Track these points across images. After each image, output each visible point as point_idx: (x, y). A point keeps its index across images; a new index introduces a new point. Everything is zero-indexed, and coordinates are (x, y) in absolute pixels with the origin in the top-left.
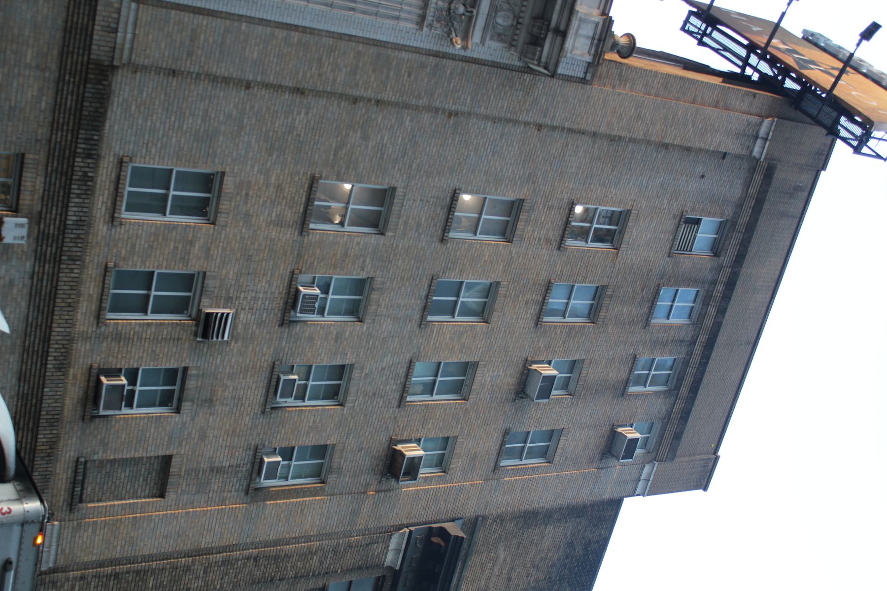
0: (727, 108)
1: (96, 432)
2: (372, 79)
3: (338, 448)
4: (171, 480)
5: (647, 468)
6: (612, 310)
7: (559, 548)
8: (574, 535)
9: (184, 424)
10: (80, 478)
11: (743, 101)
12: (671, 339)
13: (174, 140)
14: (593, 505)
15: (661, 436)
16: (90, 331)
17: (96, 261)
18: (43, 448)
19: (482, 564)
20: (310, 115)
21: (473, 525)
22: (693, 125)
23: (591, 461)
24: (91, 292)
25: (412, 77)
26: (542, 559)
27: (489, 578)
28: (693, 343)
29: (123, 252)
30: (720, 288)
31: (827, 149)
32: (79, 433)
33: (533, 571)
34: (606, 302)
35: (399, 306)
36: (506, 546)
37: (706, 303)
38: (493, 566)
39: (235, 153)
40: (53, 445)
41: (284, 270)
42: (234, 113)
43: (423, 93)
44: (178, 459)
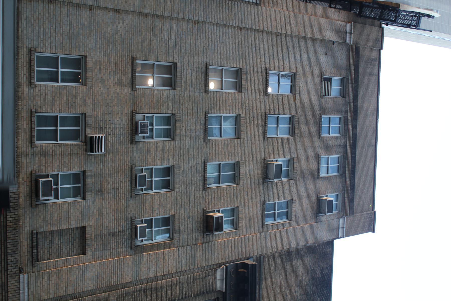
0: (328, 18)
1: (40, 214)
2: (153, 4)
3: (177, 217)
4: (88, 242)
5: (341, 221)
6: (301, 129)
7: (308, 274)
8: (314, 265)
9: (89, 206)
10: (35, 244)
11: (334, 14)
12: (334, 144)
13: (57, 38)
14: (319, 245)
15: (344, 202)
16: (28, 151)
17: (25, 108)
18: (11, 224)
19: (269, 286)
20: (125, 24)
21: (260, 259)
22: (315, 27)
23: (311, 218)
24: (25, 127)
25: (172, 3)
26: (300, 281)
27: (275, 295)
28: (345, 146)
29: (39, 103)
30: (350, 114)
31: (381, 38)
32: (30, 215)
33: (297, 289)
34: (296, 124)
35: (191, 130)
36: (279, 274)
37: (346, 124)
38: (275, 287)
39: (90, 46)
40: (17, 221)
41: (127, 111)
42: (86, 23)
43: (179, 11)
44: (90, 229)
